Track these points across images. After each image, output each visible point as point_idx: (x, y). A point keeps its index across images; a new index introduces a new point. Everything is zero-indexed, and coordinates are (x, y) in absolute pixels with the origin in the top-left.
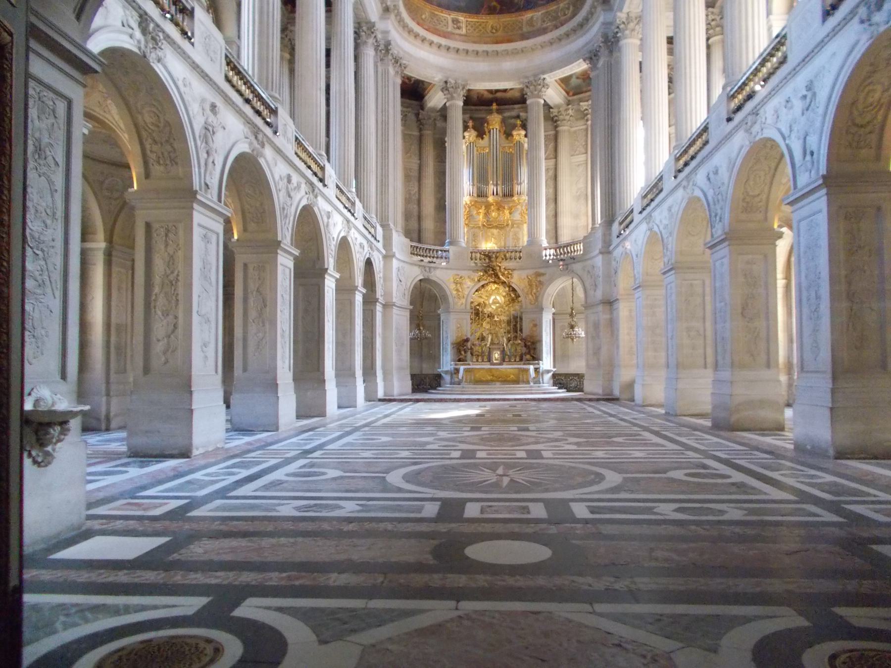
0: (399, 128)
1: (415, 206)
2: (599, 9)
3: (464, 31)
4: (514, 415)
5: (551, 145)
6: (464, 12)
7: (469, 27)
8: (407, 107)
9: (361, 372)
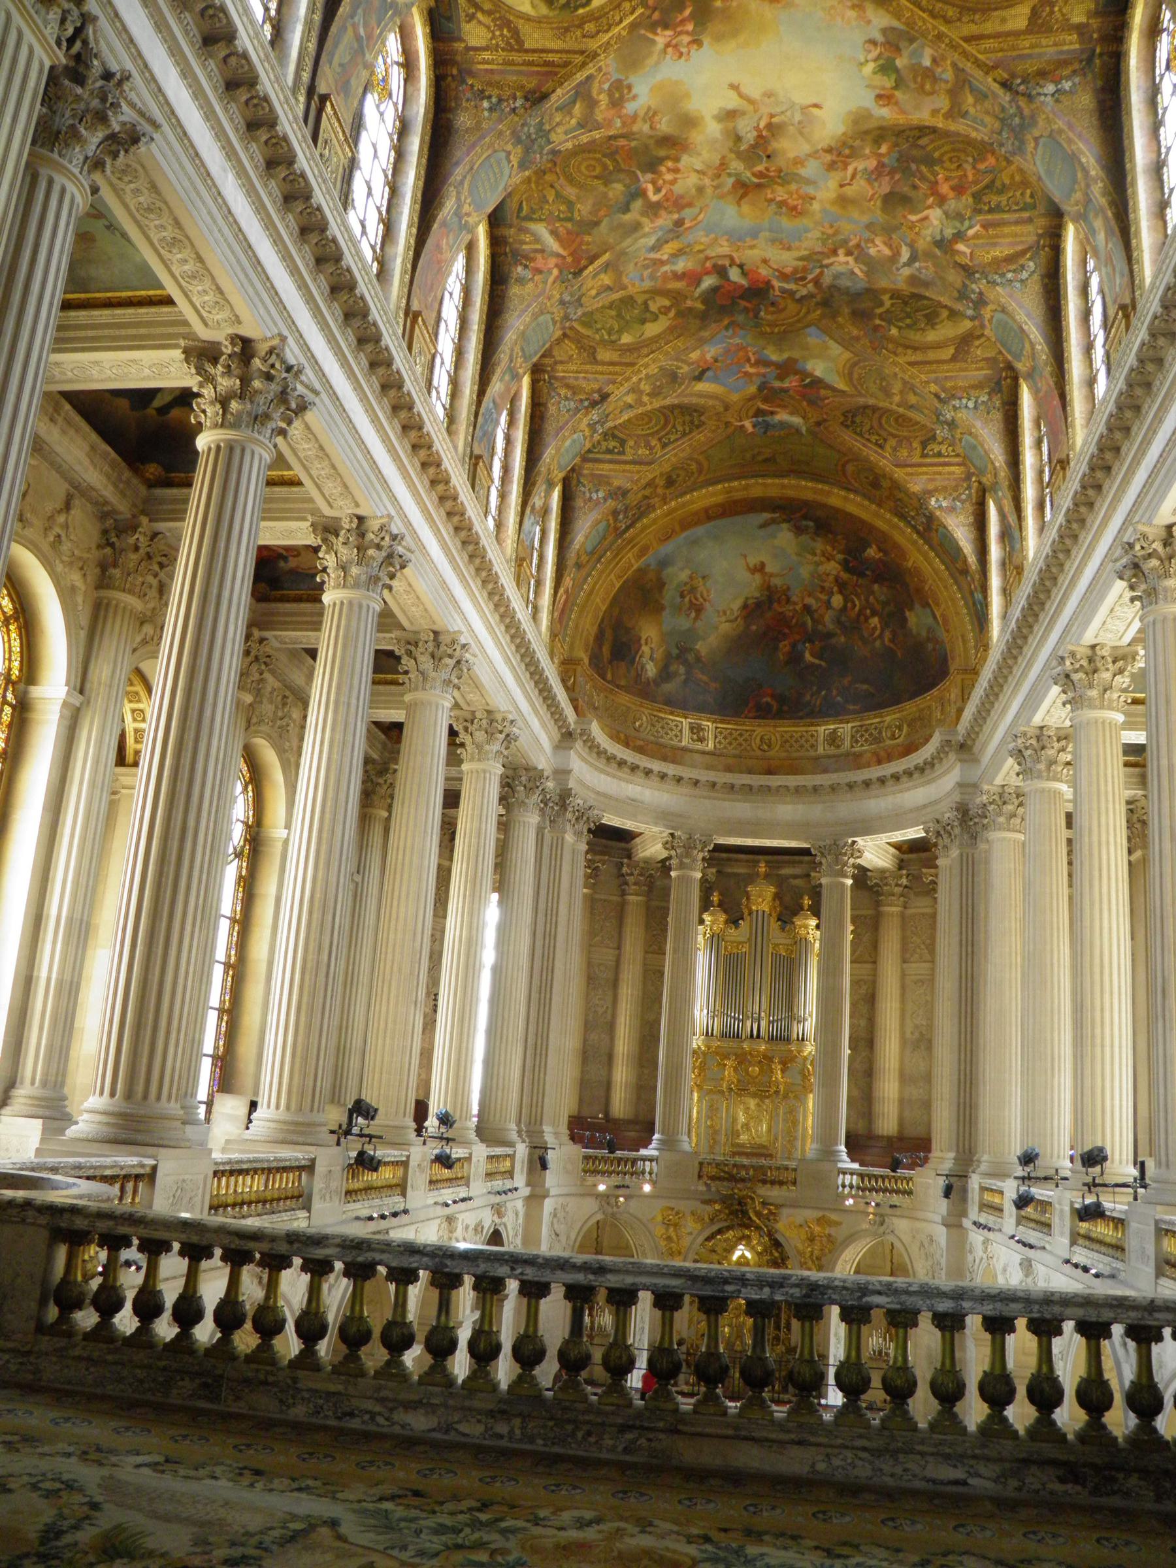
0: (581, 891)
2: (952, 756)
3: (711, 746)
5: (866, 938)
7: (719, 738)
8: (603, 853)
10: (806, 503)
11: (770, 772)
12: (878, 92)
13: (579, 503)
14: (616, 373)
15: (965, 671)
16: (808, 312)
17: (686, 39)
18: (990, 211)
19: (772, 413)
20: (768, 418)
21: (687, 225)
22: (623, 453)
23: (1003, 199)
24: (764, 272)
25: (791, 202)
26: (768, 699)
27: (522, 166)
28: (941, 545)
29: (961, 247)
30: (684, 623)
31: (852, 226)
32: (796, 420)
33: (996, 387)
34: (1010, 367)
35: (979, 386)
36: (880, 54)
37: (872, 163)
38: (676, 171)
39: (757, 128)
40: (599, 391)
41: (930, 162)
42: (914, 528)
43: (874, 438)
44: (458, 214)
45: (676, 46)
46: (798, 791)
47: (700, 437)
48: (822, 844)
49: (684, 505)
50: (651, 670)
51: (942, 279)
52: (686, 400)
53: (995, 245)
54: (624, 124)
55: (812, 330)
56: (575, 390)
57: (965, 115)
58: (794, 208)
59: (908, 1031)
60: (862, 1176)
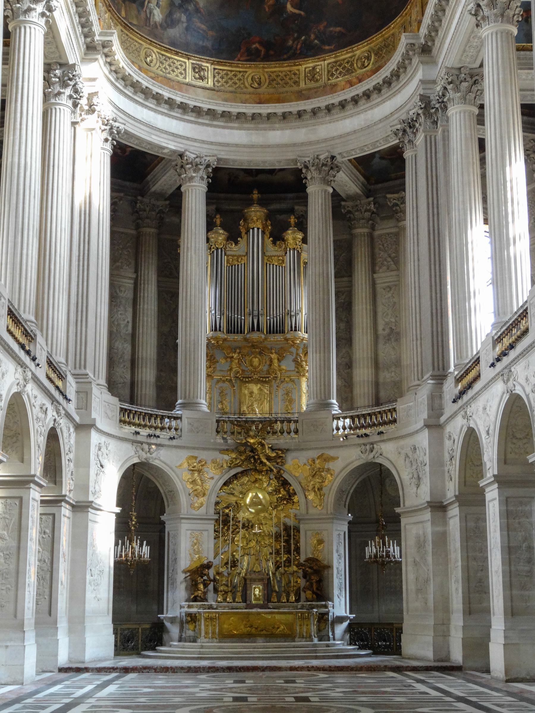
3: (210, 84)
4: (298, 699)
9: (33, 621)
26: (257, 45)
46: (285, 116)
48: (307, 159)
50: (158, 15)
59: (380, 328)
60: (352, 418)
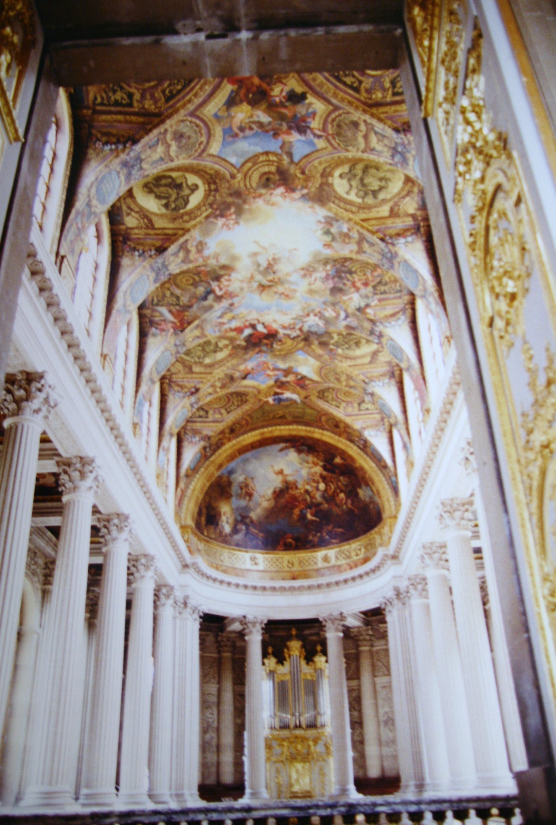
1: (214, 735)
2: (389, 562)
3: (261, 567)
5: (353, 666)
6: (262, 549)
7: (266, 562)
10: (302, 438)
11: (294, 578)
12: (324, 243)
13: (185, 444)
14: (204, 378)
15: (391, 517)
16: (298, 344)
17: (232, 222)
18: (382, 293)
19: (282, 394)
20: (280, 396)
21: (236, 305)
22: (207, 417)
23: (386, 288)
24: (275, 326)
25: (286, 293)
26: (290, 540)
27: (155, 281)
28: (372, 454)
29: (369, 310)
30: (243, 503)
31: (316, 303)
32: (295, 397)
33: (392, 375)
34: (398, 365)
35: (384, 375)
36: (324, 227)
37: (324, 274)
38: (229, 280)
39: (268, 260)
40: (195, 387)
41: (351, 272)
42: (358, 447)
43: (334, 403)
44: (124, 305)
45: (227, 226)
46: (310, 588)
47: (246, 407)
49: (240, 442)
51: (362, 326)
52: (238, 390)
53: (385, 309)
54: (204, 260)
55: (300, 352)
56: (182, 387)
57: (364, 252)
58: (287, 296)
59: (381, 715)
